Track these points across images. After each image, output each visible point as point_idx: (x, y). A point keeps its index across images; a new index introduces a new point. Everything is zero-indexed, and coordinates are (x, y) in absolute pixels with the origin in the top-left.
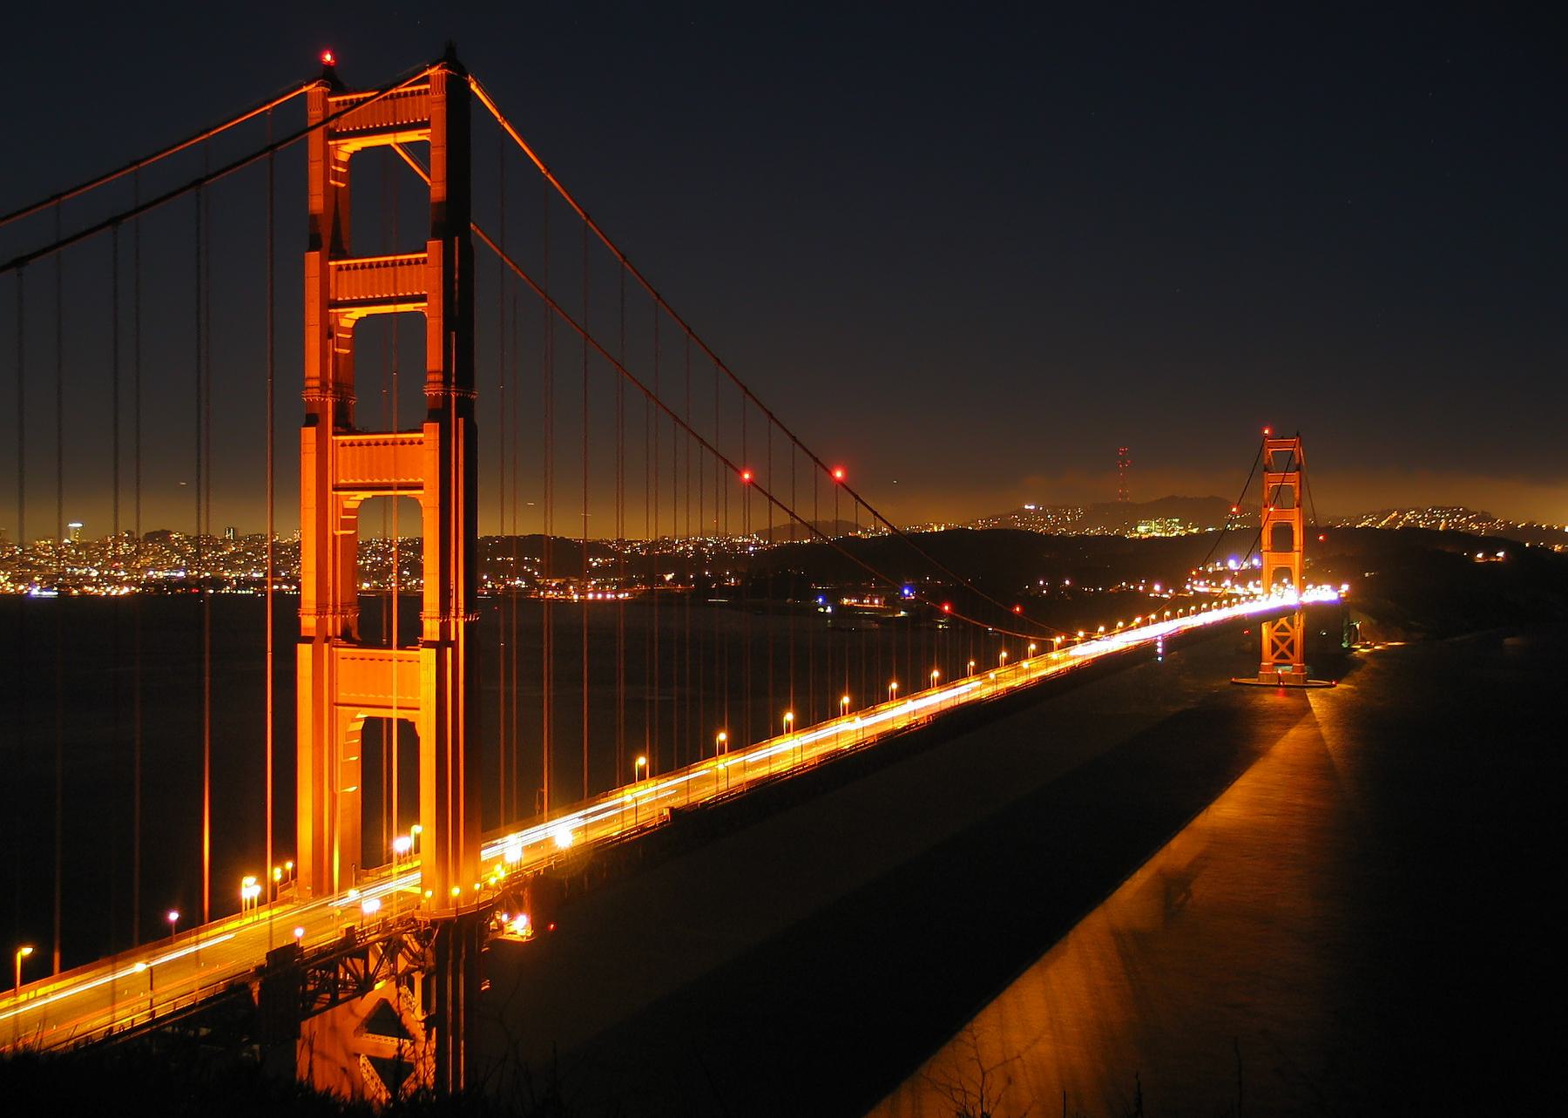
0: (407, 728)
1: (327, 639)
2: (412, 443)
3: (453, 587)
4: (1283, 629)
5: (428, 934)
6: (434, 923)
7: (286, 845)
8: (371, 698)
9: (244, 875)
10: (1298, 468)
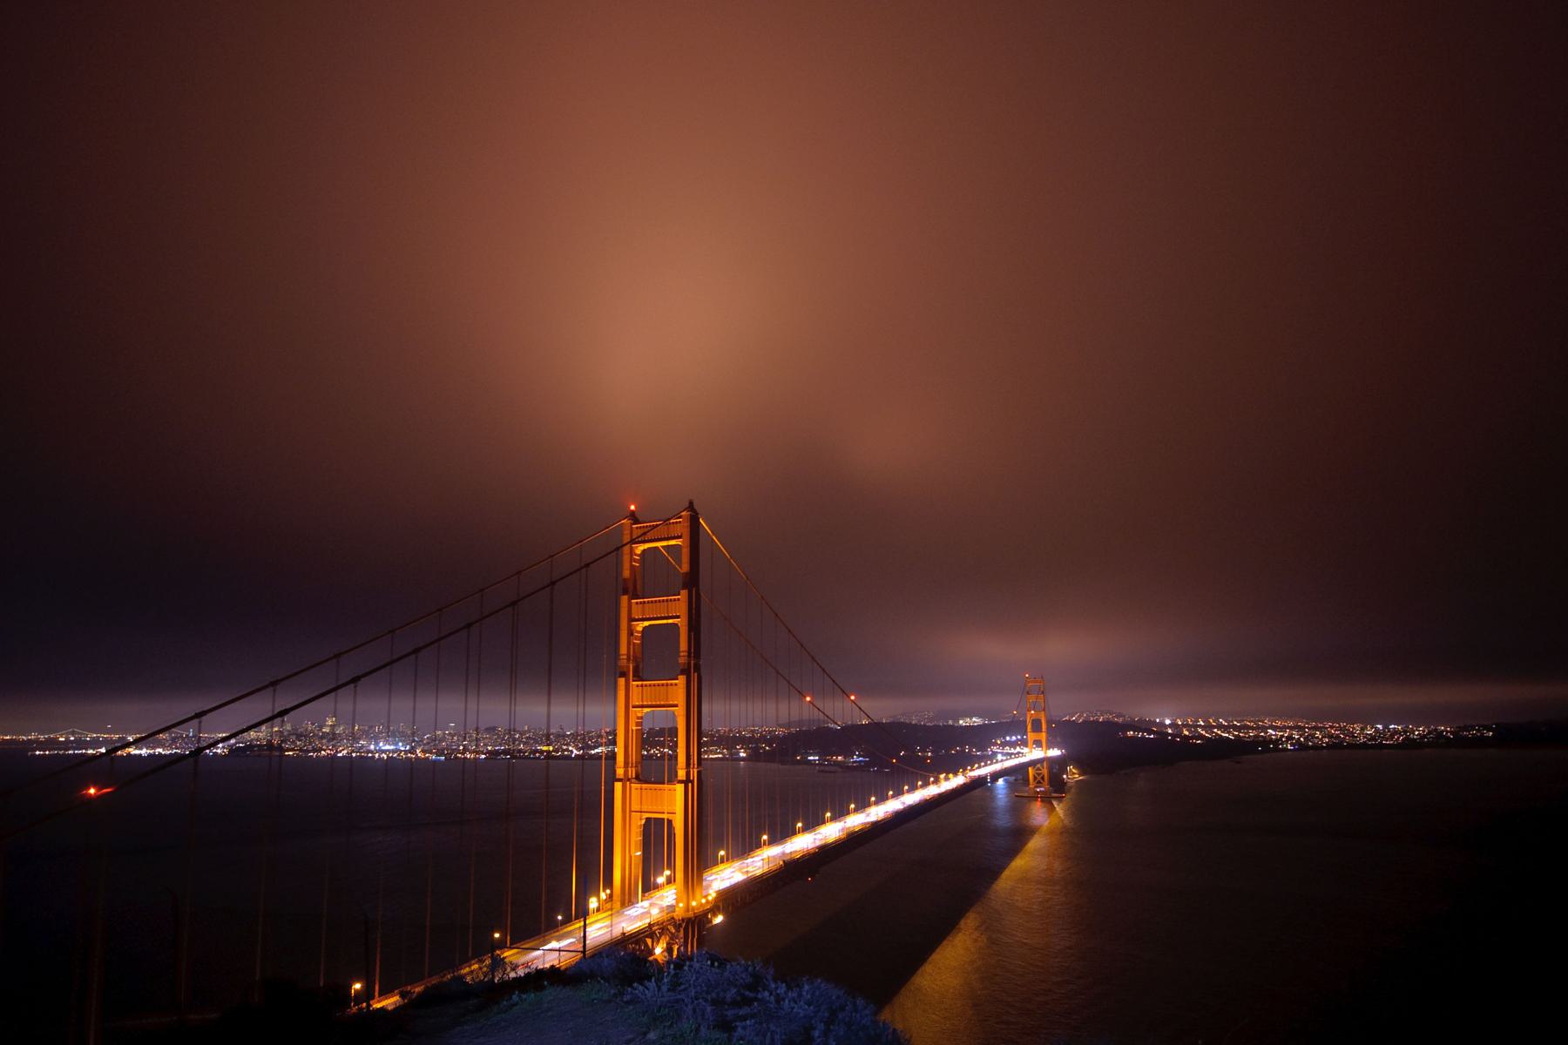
0: (670, 822)
1: (629, 780)
2: (671, 685)
3: (692, 754)
4: (1039, 769)
5: (680, 925)
6: (683, 920)
7: (609, 883)
8: (650, 809)
9: (590, 897)
10: (1043, 693)
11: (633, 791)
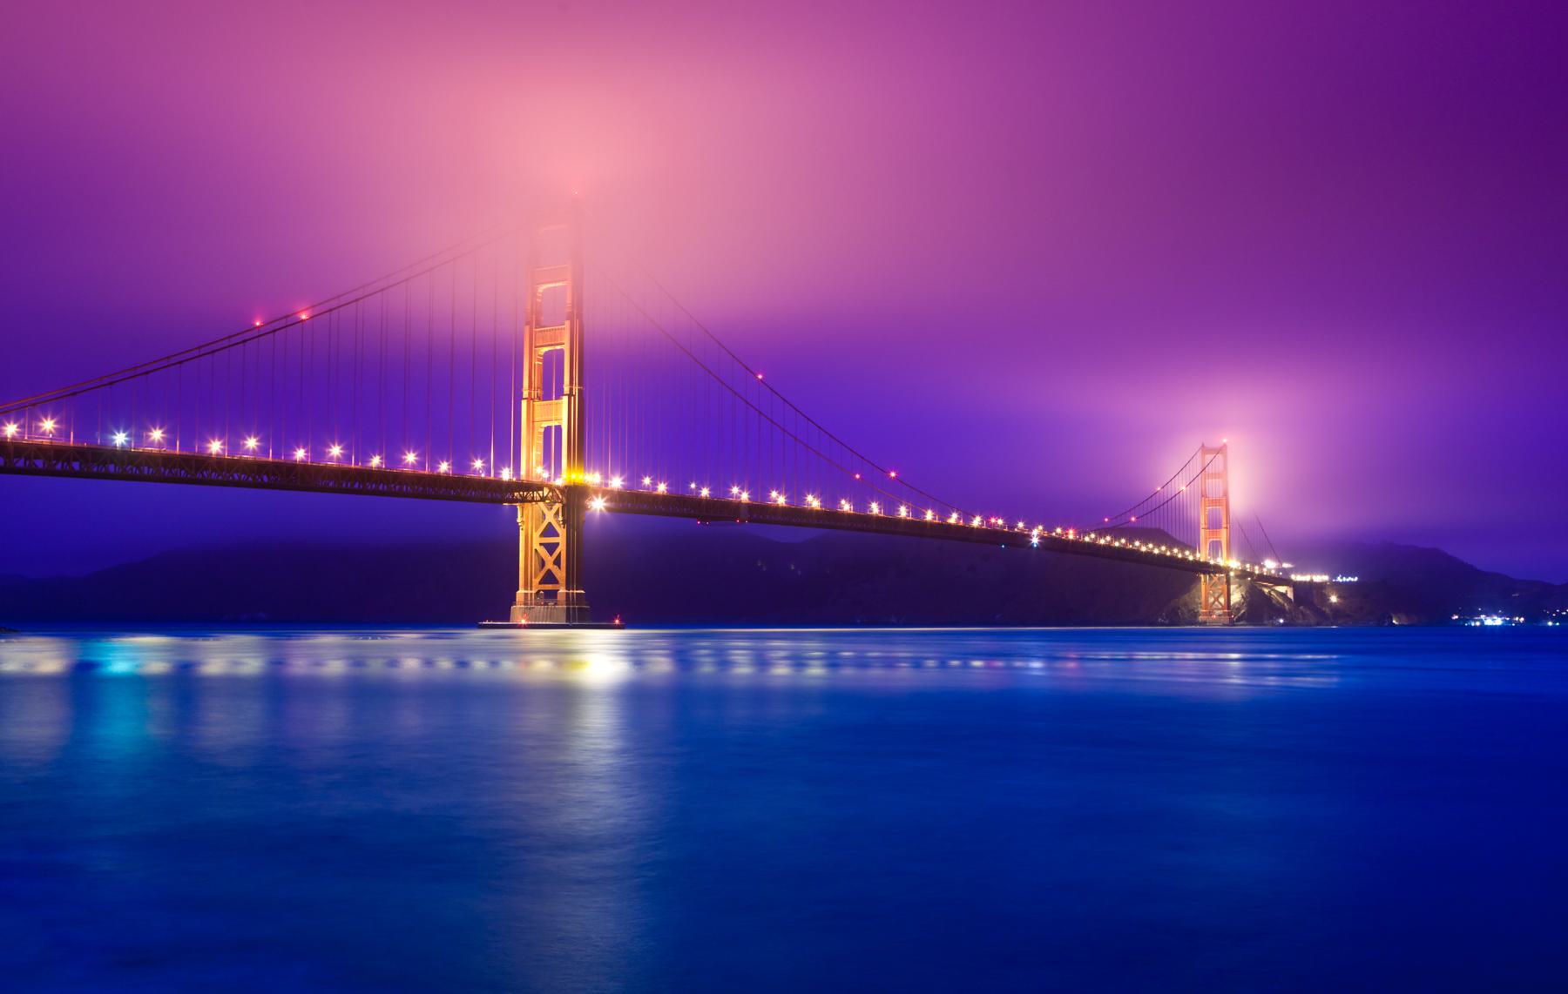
0: (558, 429)
8: (546, 418)
11: (536, 408)
